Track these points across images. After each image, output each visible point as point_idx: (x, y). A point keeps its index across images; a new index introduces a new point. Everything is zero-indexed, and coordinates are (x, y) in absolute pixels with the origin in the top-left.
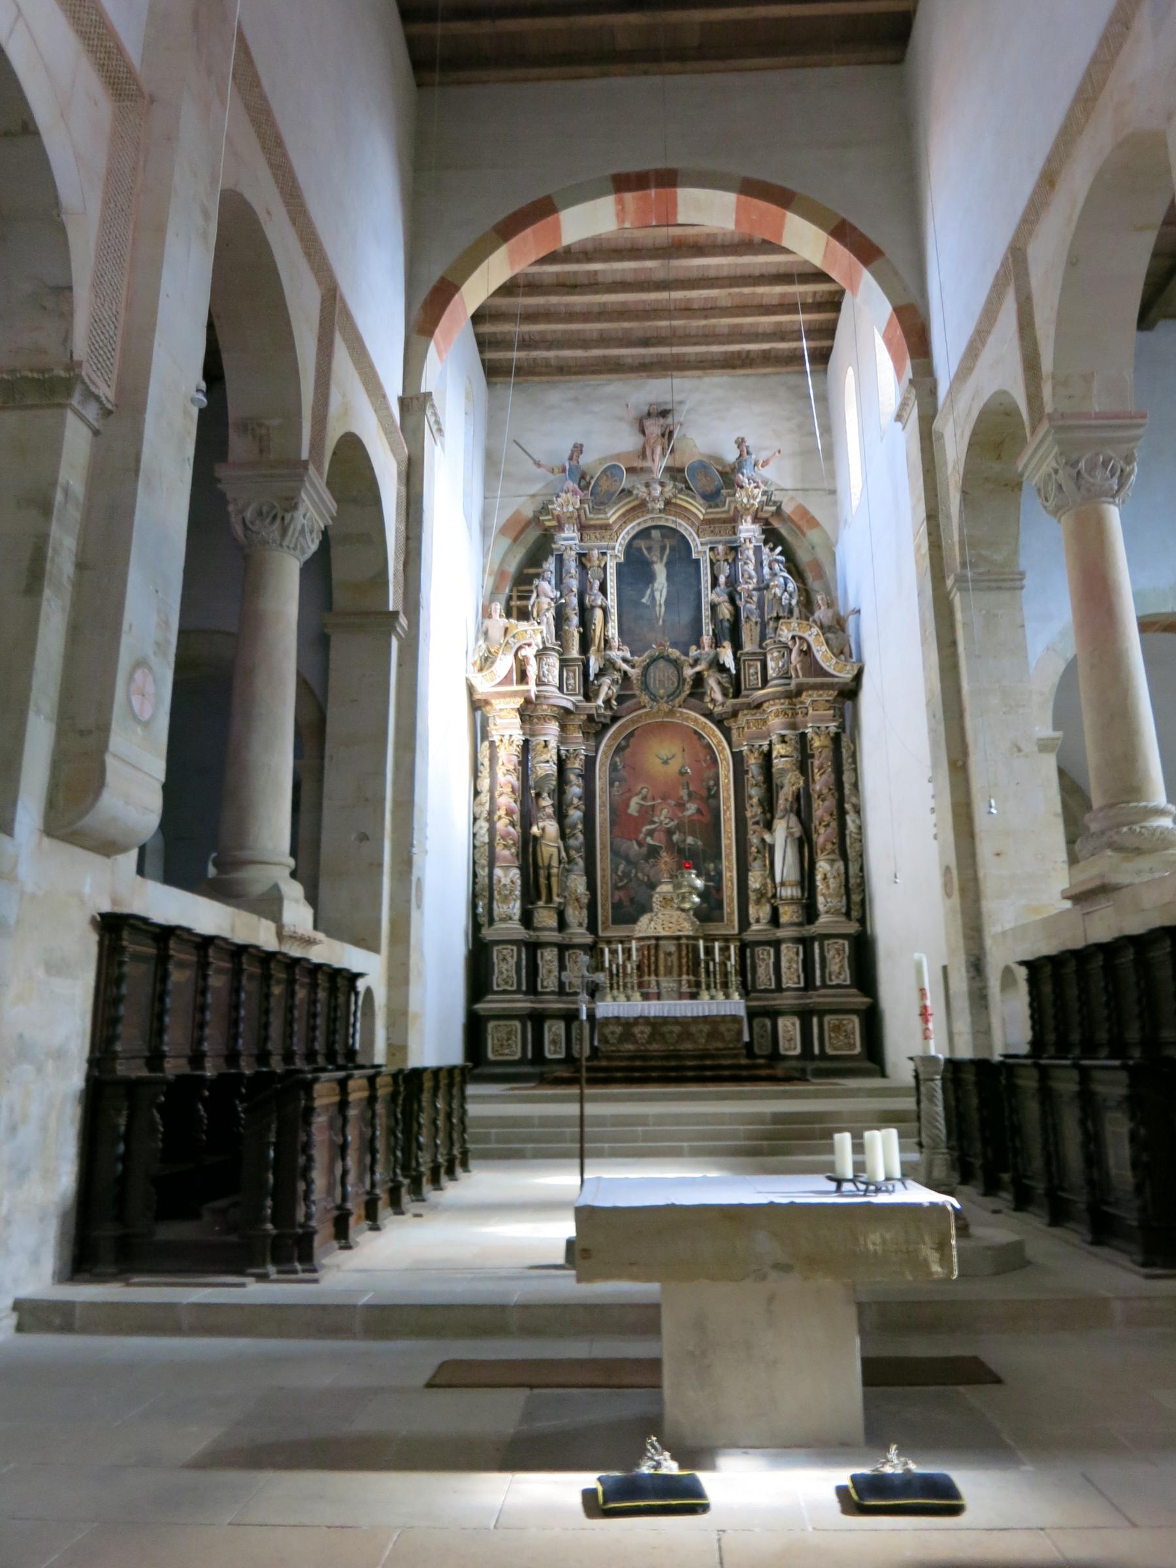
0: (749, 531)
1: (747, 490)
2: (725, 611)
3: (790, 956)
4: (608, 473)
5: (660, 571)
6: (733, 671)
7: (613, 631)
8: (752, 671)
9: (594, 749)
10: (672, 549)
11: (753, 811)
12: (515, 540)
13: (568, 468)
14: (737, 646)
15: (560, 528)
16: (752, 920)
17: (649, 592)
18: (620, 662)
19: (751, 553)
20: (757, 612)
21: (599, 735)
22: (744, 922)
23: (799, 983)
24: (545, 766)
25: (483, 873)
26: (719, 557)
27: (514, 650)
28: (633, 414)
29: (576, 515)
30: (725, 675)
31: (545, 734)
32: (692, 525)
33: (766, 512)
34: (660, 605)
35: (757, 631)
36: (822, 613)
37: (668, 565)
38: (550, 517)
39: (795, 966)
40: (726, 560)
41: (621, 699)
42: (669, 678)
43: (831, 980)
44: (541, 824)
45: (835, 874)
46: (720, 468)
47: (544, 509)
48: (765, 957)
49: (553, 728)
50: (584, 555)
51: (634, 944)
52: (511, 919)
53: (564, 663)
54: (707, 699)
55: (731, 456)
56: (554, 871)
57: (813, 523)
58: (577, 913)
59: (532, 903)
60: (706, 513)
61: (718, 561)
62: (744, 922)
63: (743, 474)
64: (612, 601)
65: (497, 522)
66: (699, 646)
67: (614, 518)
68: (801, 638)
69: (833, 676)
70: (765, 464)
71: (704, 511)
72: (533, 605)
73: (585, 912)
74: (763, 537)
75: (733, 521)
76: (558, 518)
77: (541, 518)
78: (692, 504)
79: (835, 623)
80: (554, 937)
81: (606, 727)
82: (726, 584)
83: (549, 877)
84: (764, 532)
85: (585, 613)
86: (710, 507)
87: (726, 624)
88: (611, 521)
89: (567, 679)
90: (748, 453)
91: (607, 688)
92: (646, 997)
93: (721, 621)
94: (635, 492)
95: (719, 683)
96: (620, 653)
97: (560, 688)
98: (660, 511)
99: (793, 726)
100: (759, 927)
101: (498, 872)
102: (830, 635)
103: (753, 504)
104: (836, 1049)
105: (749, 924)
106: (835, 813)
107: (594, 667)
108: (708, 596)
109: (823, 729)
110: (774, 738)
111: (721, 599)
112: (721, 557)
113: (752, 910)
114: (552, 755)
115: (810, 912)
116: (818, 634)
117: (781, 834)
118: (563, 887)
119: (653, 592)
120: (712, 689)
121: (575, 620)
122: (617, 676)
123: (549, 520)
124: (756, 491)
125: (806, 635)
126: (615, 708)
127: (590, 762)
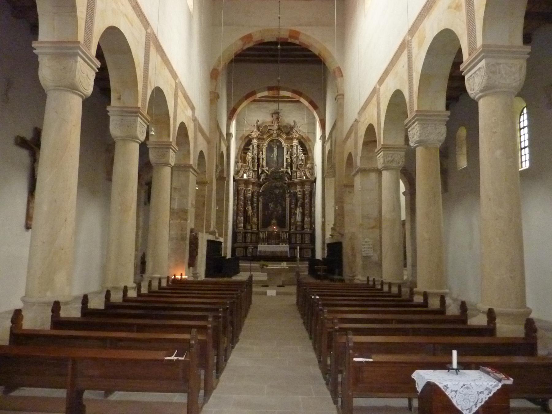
0: (295, 142)
2: (289, 160)
3: (299, 237)
5: (275, 149)
8: (294, 175)
11: (293, 206)
13: (255, 125)
14: (291, 169)
15: (253, 138)
16: (291, 229)
17: (273, 154)
18: (266, 171)
19: (295, 148)
20: (296, 161)
22: (290, 230)
24: (249, 195)
25: (235, 217)
28: (271, 112)
35: (296, 165)
36: (309, 166)
41: (265, 179)
44: (248, 207)
46: (289, 127)
47: (249, 135)
48: (293, 236)
49: (251, 186)
50: (258, 145)
51: (266, 233)
53: (254, 171)
55: (292, 124)
57: (310, 140)
62: (290, 230)
64: (264, 156)
66: (283, 168)
69: (310, 179)
70: (299, 127)
73: (256, 226)
75: (292, 139)
76: (253, 137)
80: (250, 231)
81: (262, 185)
82: (290, 154)
83: (249, 218)
84: (299, 142)
85: (258, 159)
86: (287, 136)
87: (289, 163)
90: (296, 124)
91: (263, 177)
92: (268, 244)
97: (253, 177)
98: (276, 136)
99: (302, 188)
101: (239, 217)
102: (310, 170)
107: (260, 171)
108: (286, 156)
110: (298, 191)
114: (250, 192)
115: (303, 228)
117: (298, 211)
118: (252, 220)
119: (273, 154)
121: (256, 161)
125: (305, 170)
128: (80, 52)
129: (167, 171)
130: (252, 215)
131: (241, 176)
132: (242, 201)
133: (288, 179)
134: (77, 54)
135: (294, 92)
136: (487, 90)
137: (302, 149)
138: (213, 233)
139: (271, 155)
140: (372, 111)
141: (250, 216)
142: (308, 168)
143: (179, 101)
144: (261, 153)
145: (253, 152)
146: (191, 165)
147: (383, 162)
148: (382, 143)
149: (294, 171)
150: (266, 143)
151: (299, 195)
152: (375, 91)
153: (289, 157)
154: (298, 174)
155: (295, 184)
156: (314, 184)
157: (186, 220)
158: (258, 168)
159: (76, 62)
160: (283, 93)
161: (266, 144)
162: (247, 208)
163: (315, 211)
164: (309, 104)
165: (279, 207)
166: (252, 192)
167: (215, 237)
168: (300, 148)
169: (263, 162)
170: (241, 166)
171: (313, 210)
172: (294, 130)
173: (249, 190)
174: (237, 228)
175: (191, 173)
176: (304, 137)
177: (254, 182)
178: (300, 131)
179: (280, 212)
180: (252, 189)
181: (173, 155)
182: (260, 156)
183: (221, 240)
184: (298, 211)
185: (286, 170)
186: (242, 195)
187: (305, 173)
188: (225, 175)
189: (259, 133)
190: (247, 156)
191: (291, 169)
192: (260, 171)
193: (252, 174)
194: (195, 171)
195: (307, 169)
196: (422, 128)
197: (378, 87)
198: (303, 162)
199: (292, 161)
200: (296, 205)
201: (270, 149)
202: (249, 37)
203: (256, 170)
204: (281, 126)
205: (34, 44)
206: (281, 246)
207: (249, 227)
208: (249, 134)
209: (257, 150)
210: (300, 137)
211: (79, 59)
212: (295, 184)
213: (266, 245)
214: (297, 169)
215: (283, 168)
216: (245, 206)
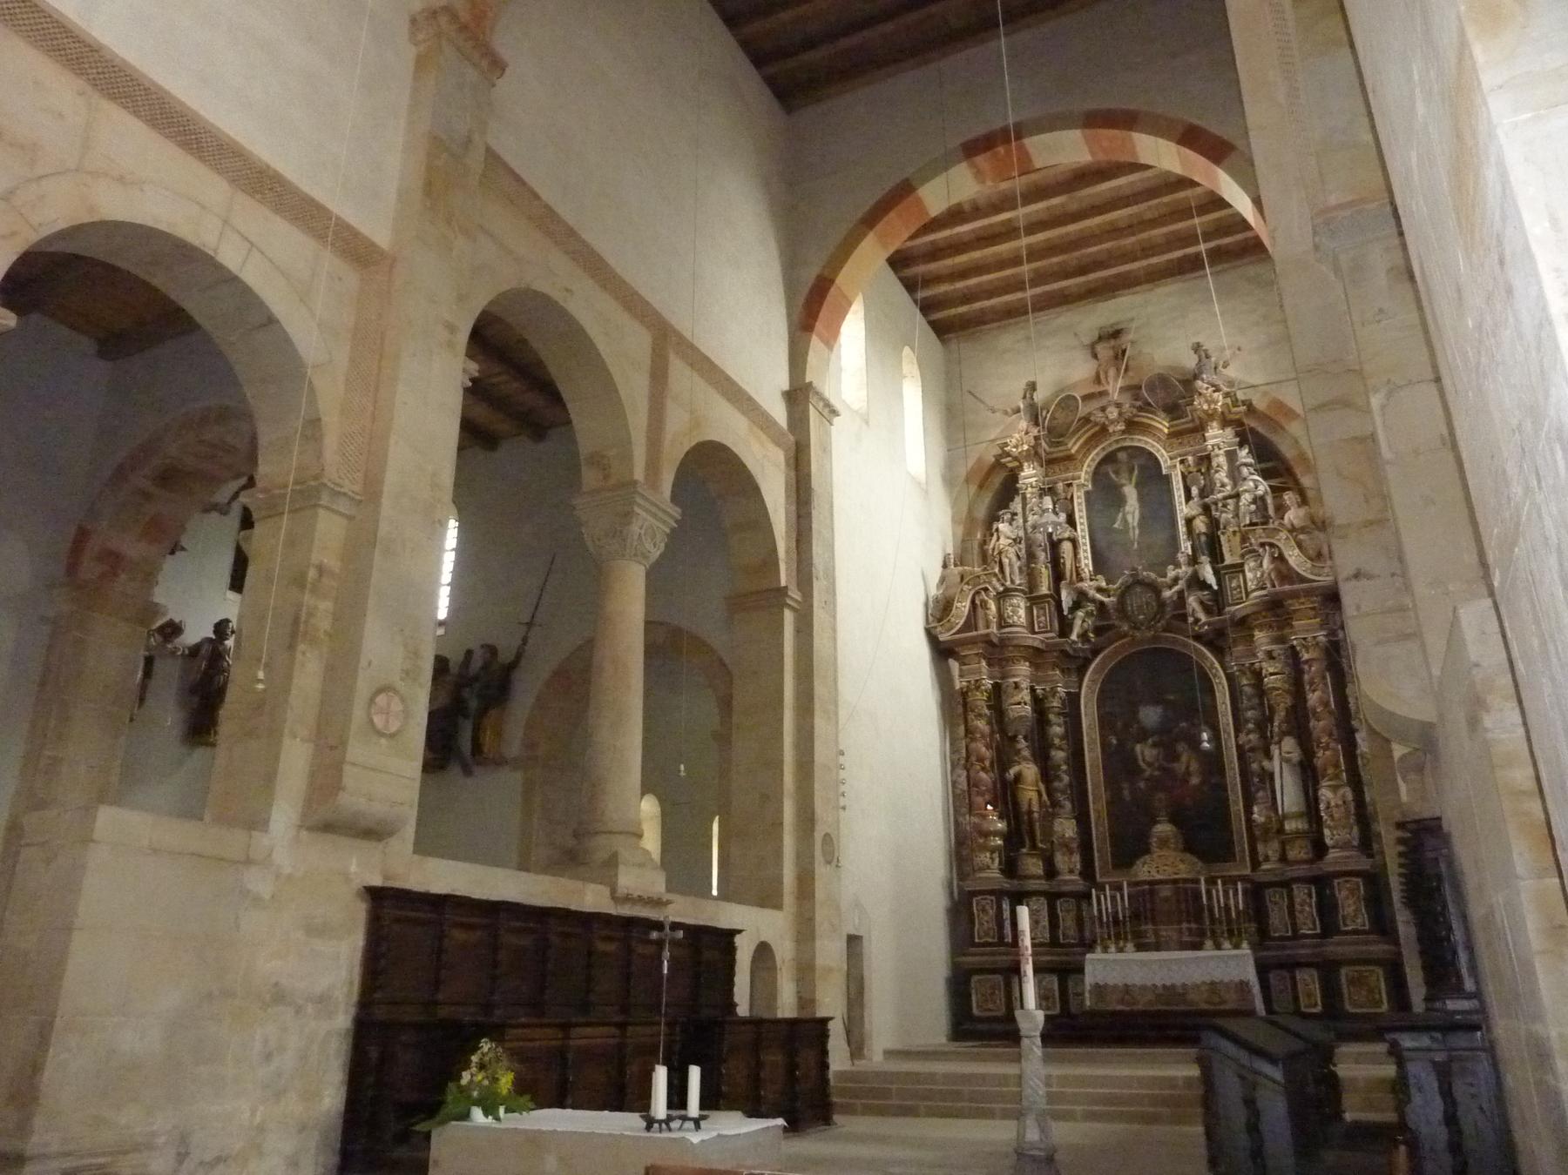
0: (1217, 437)
1: (1205, 397)
2: (1200, 525)
4: (1063, 405)
5: (1130, 492)
6: (1216, 587)
7: (1087, 563)
8: (1234, 584)
9: (1077, 685)
10: (1142, 468)
12: (981, 487)
13: (1022, 406)
14: (1216, 556)
15: (1021, 468)
17: (1120, 515)
18: (1092, 593)
21: (1082, 671)
23: (1315, 929)
24: (1020, 707)
26: (1191, 469)
27: (970, 597)
28: (1087, 340)
29: (1033, 452)
30: (1206, 593)
31: (1014, 676)
32: (1159, 440)
33: (1237, 413)
34: (1134, 528)
37: (1137, 486)
38: (1009, 459)
39: (1307, 909)
40: (1199, 471)
41: (1098, 631)
42: (1147, 603)
43: (1346, 925)
45: (1340, 802)
46: (1180, 377)
48: (1275, 899)
52: (988, 868)
53: (1034, 600)
54: (1191, 620)
55: (1190, 362)
56: (1036, 815)
58: (1066, 859)
59: (1018, 850)
60: (1171, 426)
61: (1190, 473)
63: (1203, 380)
65: (962, 471)
67: (1076, 448)
69: (1314, 581)
70: (1225, 367)
71: (1167, 425)
72: (994, 549)
73: (1077, 858)
74: (1238, 439)
75: (1199, 429)
76: (1016, 459)
77: (1003, 460)
78: (1154, 420)
79: (1309, 523)
81: (1087, 662)
83: (1031, 823)
84: (1237, 434)
86: (1172, 420)
87: (1203, 538)
88: (1073, 451)
89: (1038, 617)
90: (1208, 357)
91: (1081, 622)
92: (1140, 947)
93: (1199, 535)
94: (1092, 418)
95: (1201, 603)
96: (1093, 583)
98: (1123, 432)
99: (1281, 640)
102: (1301, 537)
103: (1215, 409)
104: (1355, 1005)
105: (1259, 864)
106: (1335, 732)
107: (1066, 598)
108: (1183, 509)
109: (1309, 639)
111: (1194, 513)
113: (1260, 847)
114: (1025, 695)
115: (1320, 849)
116: (1287, 538)
118: (1048, 832)
119: (1124, 515)
120: (1194, 610)
122: (1091, 607)
123: (1010, 462)
124: (1216, 394)
126: (1093, 640)
127: (1073, 700)
132: (983, 736)
133: (1208, 610)
141: (1035, 808)
142: (1293, 530)
150: (1083, 474)
151: (1274, 676)
154: (1249, 575)
161: (1084, 475)
165: (1184, 758)
167: (606, 891)
169: (1076, 554)
173: (1017, 686)
179: (1195, 780)
180: (1035, 679)
191: (1216, 556)
192: (1066, 598)
193: (1022, 612)
195: (1283, 535)
199: (1214, 524)
201: (1105, 494)
203: (1046, 596)
206: (1212, 958)
212: (1243, 623)
213: (1131, 954)
215: (1177, 565)
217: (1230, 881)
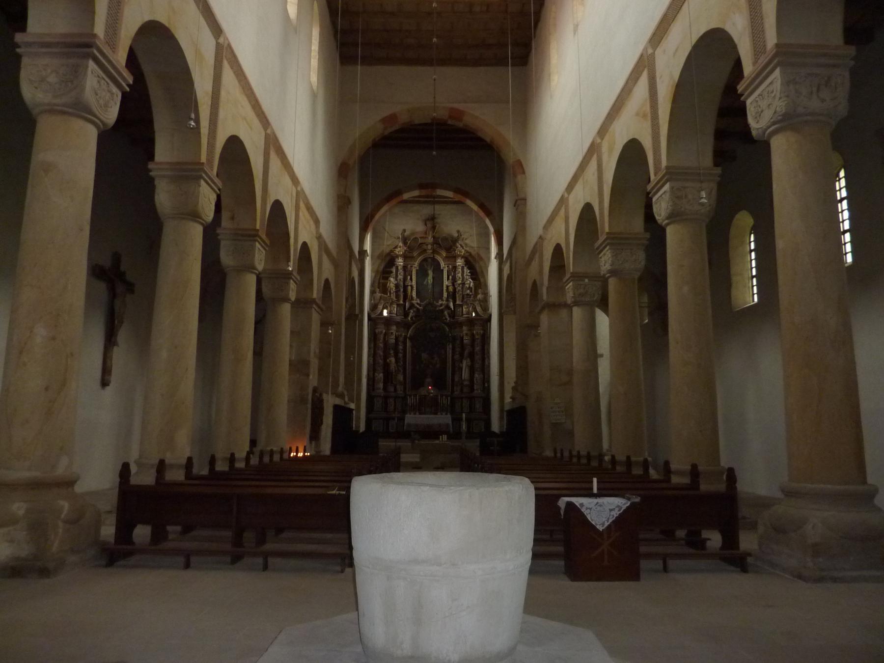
0: (460, 262)
2: (451, 289)
3: (466, 403)
5: (430, 273)
6: (453, 309)
7: (414, 294)
11: (457, 357)
15: (397, 256)
17: (426, 280)
18: (416, 305)
19: (460, 270)
20: (461, 290)
24: (392, 341)
32: (441, 258)
36: (480, 296)
40: (452, 270)
41: (416, 316)
44: (390, 359)
47: (392, 251)
49: (394, 328)
52: (380, 389)
53: (398, 305)
55: (456, 235)
57: (481, 259)
62: (453, 391)
64: (414, 283)
68: (472, 304)
69: (481, 316)
70: (466, 240)
75: (455, 258)
76: (397, 255)
81: (410, 326)
82: (452, 279)
84: (465, 261)
85: (405, 287)
87: (451, 293)
90: (461, 235)
91: (412, 313)
92: (420, 414)
97: (397, 315)
99: (470, 330)
100: (457, 393)
101: (376, 374)
102: (481, 303)
105: (454, 392)
107: (407, 304)
108: (446, 283)
112: (450, 270)
113: (455, 388)
114: (393, 337)
115: (472, 390)
117: (465, 364)
119: (428, 280)
121: (402, 290)
128: (204, 175)
129: (286, 308)
130: (395, 371)
131: (380, 312)
133: (450, 316)
134: (201, 177)
135: (457, 191)
136: (674, 216)
137: (469, 273)
138: (341, 396)
139: (424, 281)
140: (559, 225)
141: (394, 371)
142: (480, 301)
143: (301, 214)
144: (409, 277)
145: (397, 276)
146: (315, 299)
147: (573, 295)
148: (571, 271)
149: (458, 304)
150: (416, 264)
151: (467, 340)
152: (563, 201)
153: (450, 284)
154: (464, 310)
155: (461, 325)
156: (489, 323)
157: (308, 375)
158: (404, 301)
159: (200, 186)
160: (440, 192)
162: (388, 360)
163: (489, 363)
164: (479, 209)
165: (436, 359)
166: (396, 336)
168: (467, 271)
170: (379, 297)
171: (486, 363)
172: (458, 244)
173: (392, 333)
174: (373, 390)
175: (313, 309)
176: (473, 253)
177: (399, 321)
178: (466, 245)
179: (438, 366)
181: (293, 287)
182: (408, 283)
183: (352, 406)
184: (465, 364)
185: (446, 303)
186: (381, 341)
187: (475, 308)
188: (357, 312)
189: (405, 248)
190: (388, 282)
191: (454, 302)
193: (395, 309)
194: (319, 307)
195: (477, 302)
196: (614, 254)
197: (566, 195)
198: (471, 291)
199: (455, 289)
200: (462, 355)
201: (422, 273)
202: (391, 119)
204: (439, 238)
205: (151, 166)
207: (392, 389)
208: (391, 250)
209: (402, 274)
210: (467, 254)
211: (202, 182)
212: (461, 325)
213: (417, 416)
214: (462, 301)
216: (385, 357)
217: (447, 396)
